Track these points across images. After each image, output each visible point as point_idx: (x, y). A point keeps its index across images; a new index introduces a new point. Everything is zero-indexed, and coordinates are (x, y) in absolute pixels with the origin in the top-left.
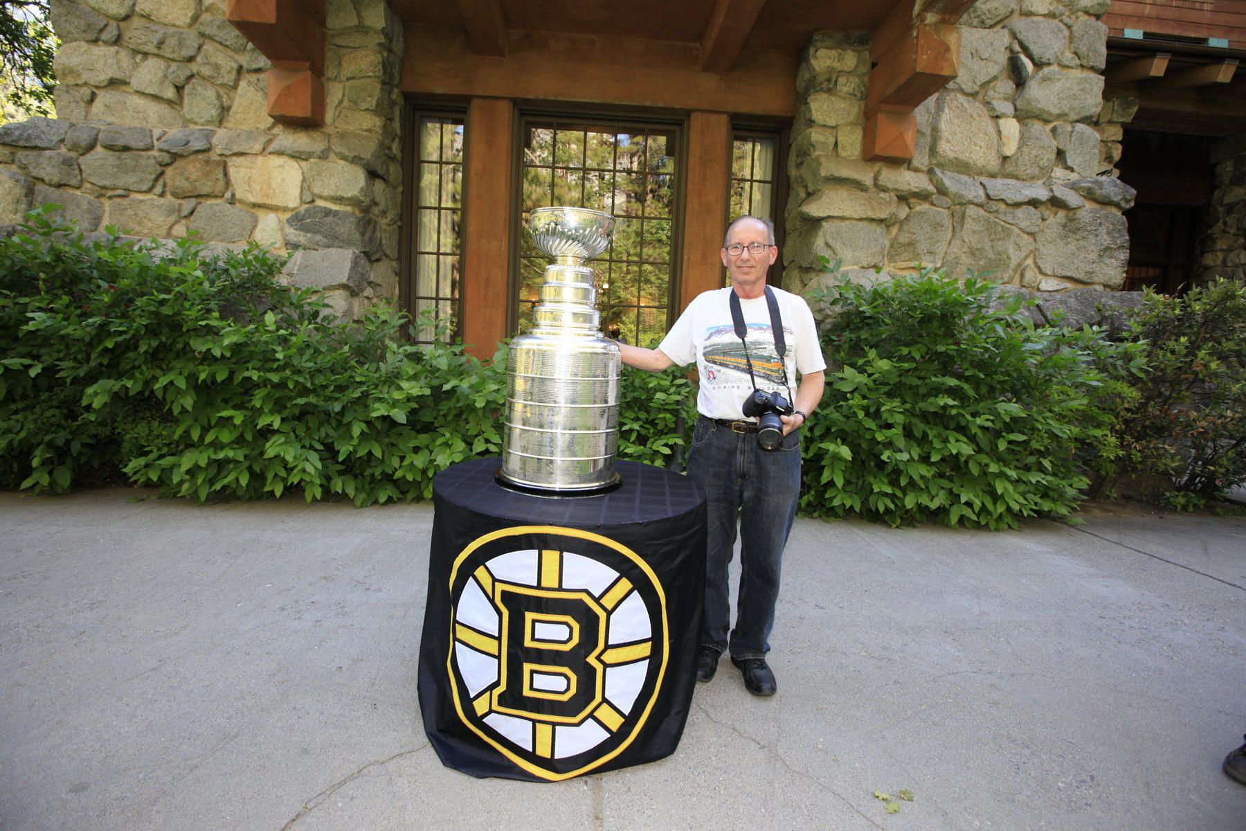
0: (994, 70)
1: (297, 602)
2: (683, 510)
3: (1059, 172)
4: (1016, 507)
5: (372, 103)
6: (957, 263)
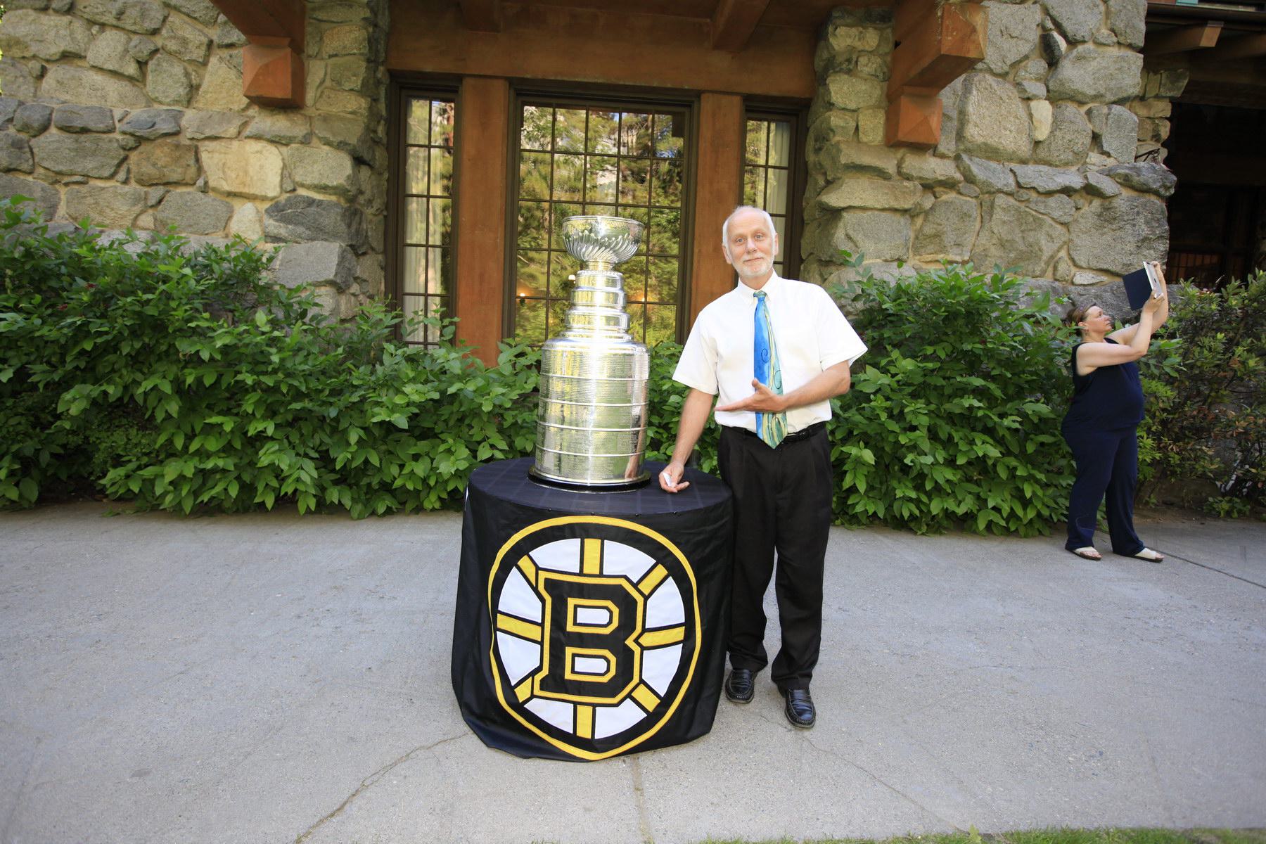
0: (1025, 48)
1: (313, 610)
2: (711, 502)
3: (1094, 158)
4: (1046, 512)
5: (356, 83)
6: (986, 256)
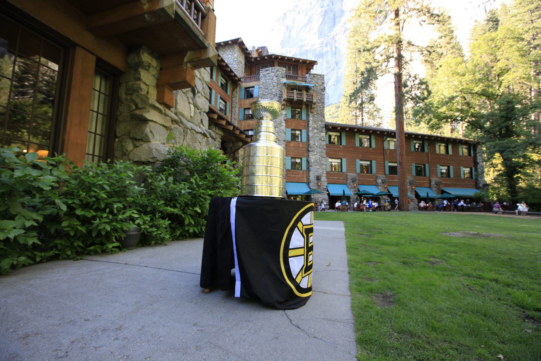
3: (202, 126)
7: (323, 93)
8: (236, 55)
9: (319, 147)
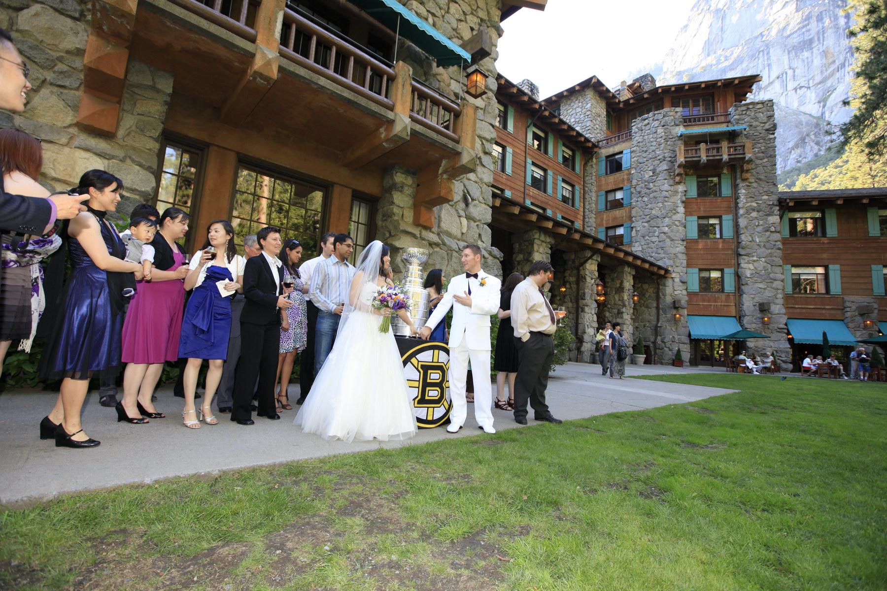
7: (772, 136)
8: (589, 105)
9: (764, 246)
